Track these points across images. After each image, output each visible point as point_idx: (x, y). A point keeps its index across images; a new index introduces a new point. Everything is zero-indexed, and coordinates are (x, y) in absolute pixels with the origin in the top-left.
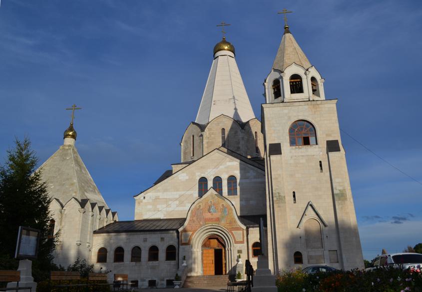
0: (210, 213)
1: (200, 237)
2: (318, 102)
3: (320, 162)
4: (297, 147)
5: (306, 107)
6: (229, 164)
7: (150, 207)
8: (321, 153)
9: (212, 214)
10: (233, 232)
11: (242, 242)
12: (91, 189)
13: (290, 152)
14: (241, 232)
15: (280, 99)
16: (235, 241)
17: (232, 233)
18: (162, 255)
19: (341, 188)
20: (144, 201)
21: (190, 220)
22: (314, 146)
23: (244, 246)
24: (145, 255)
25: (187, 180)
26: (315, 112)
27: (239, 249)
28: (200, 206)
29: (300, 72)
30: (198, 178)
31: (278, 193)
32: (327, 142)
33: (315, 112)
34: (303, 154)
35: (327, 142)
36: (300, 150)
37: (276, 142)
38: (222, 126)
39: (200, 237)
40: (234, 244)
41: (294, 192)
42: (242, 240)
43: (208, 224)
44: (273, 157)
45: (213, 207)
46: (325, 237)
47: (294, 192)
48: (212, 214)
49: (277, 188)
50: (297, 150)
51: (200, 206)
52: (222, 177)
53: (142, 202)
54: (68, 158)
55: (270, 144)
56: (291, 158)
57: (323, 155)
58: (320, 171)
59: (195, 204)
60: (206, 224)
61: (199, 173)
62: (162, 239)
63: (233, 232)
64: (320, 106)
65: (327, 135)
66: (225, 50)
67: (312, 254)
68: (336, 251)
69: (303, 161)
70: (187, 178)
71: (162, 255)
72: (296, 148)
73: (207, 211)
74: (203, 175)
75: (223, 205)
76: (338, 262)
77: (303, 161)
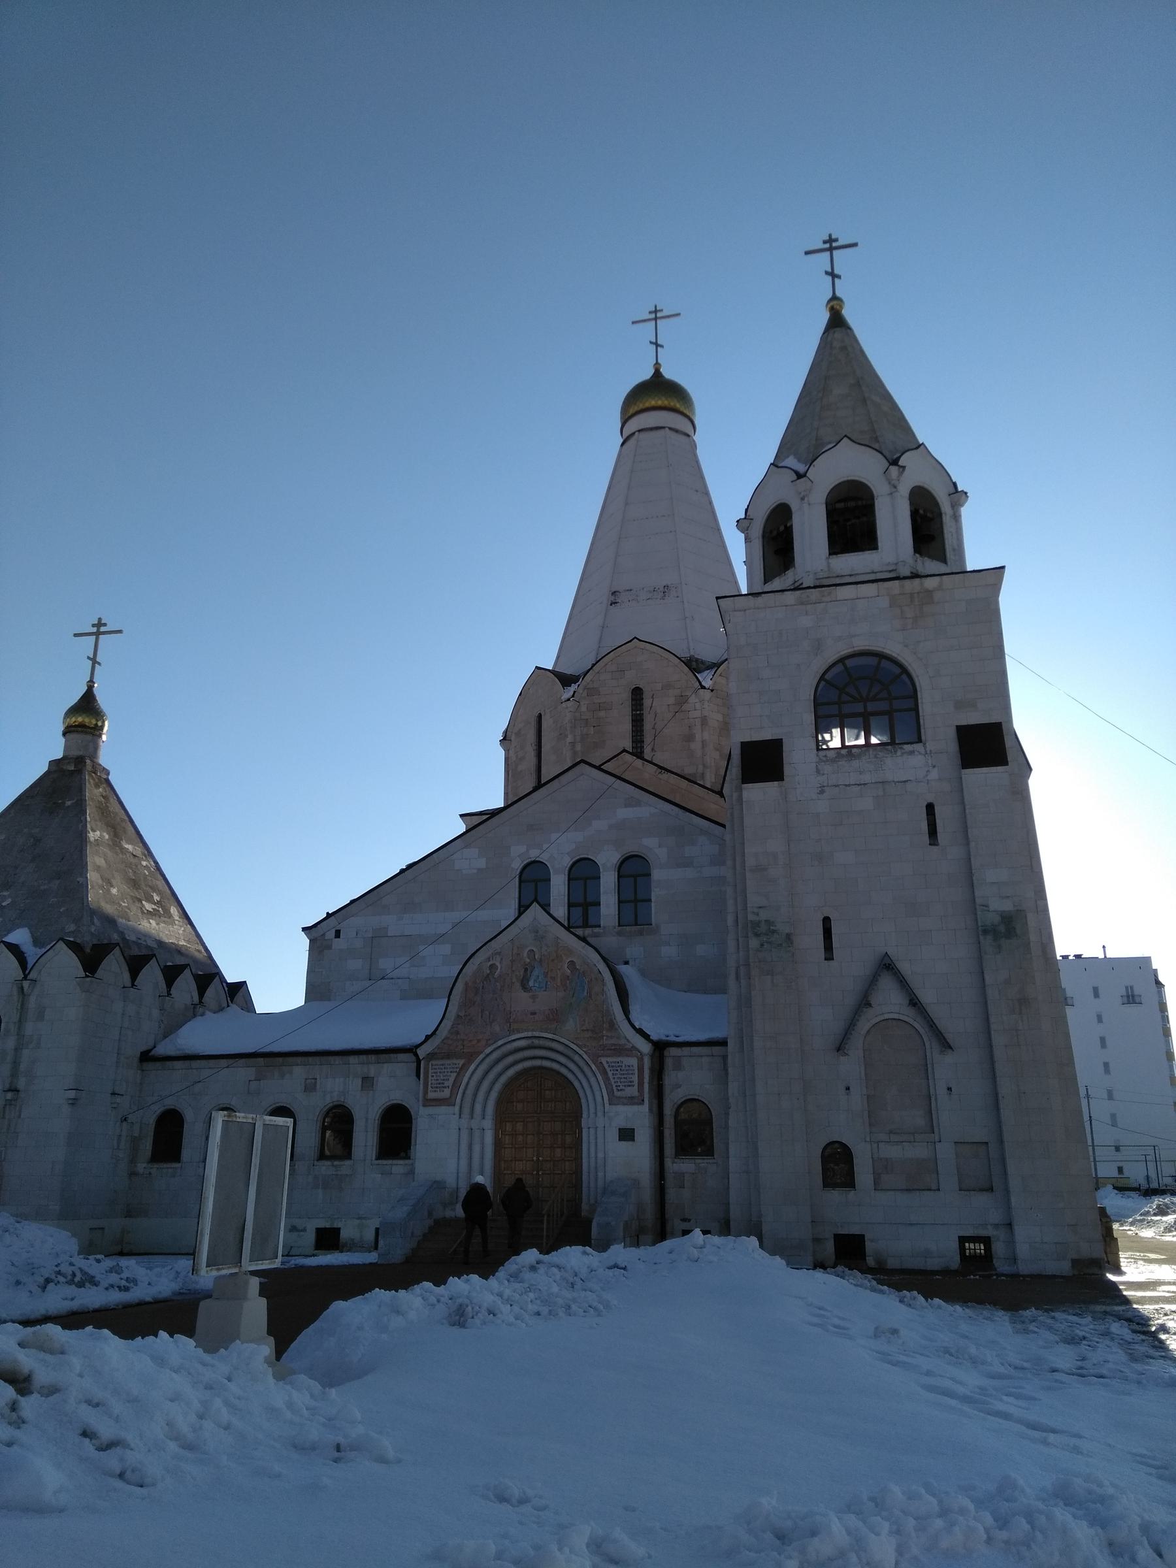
0: (525, 987)
1: (491, 1076)
2: (930, 583)
6: (623, 813)
7: (355, 964)
8: (934, 774)
9: (534, 997)
10: (604, 1060)
11: (631, 1101)
12: (148, 907)
13: (818, 771)
14: (634, 1062)
15: (788, 579)
16: (611, 1093)
17: (600, 1066)
18: (365, 1138)
19: (1007, 906)
20: (339, 944)
21: (458, 1016)
22: (907, 747)
23: (640, 1117)
25: (479, 870)
27: (624, 1125)
28: (493, 967)
30: (517, 865)
32: (960, 729)
34: (867, 778)
35: (960, 729)
37: (766, 735)
38: (632, 678)
39: (491, 1076)
40: (607, 1105)
41: (827, 921)
42: (633, 1091)
43: (519, 1032)
44: (757, 793)
45: (536, 973)
46: (941, 1091)
47: (827, 921)
48: (534, 997)
51: (493, 967)
52: (600, 860)
53: (329, 947)
54: (69, 803)
55: (744, 745)
56: (822, 792)
58: (926, 838)
60: (511, 1031)
61: (523, 849)
62: (368, 1082)
63: (604, 1060)
65: (960, 705)
67: (892, 1152)
68: (987, 1143)
70: (482, 863)
71: (365, 1138)
73: (518, 985)
74: (534, 854)
75: (572, 962)
76: (991, 1189)
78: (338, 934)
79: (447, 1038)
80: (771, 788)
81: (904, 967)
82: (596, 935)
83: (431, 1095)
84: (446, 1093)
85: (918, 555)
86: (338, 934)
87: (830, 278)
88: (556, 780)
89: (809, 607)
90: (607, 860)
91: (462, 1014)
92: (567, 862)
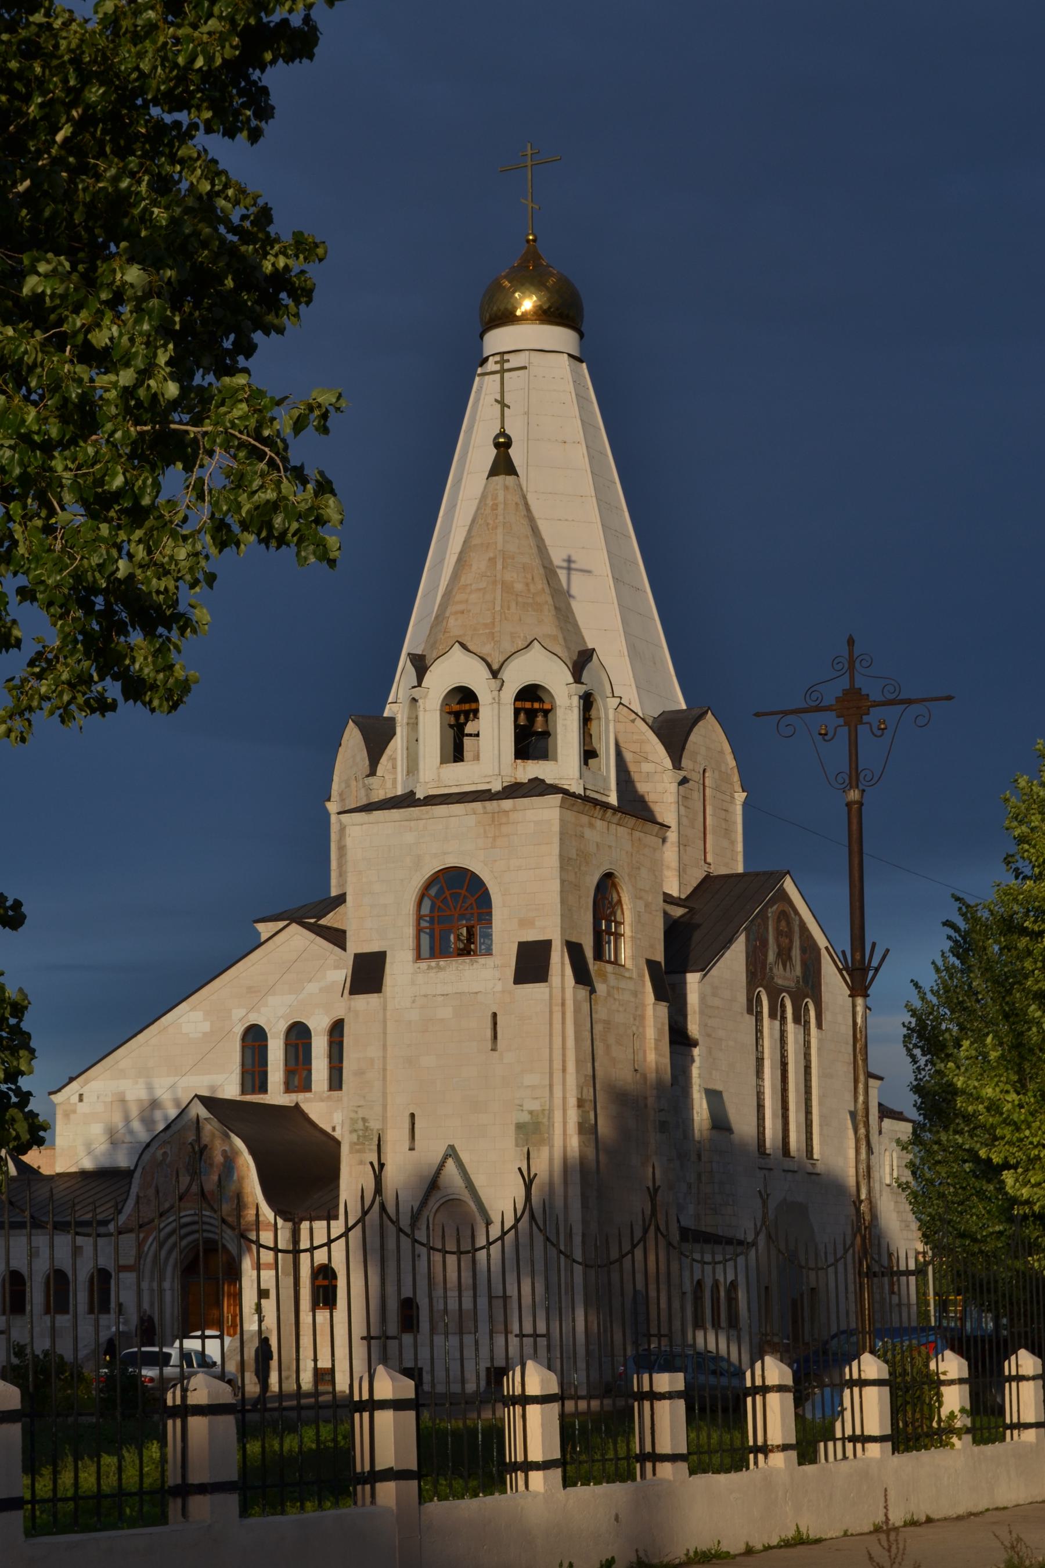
3: (495, 1015)
4: (433, 963)
5: (471, 820)
8: (499, 987)
20: (82, 1108)
24: (36, 1296)
25: (205, 1034)
26: (495, 838)
29: (478, 679)
30: (239, 1030)
31: (364, 1120)
32: (521, 945)
33: (495, 838)
35: (521, 945)
36: (441, 975)
37: (374, 947)
49: (362, 1103)
50: (432, 974)
51: (165, 1153)
53: (74, 1112)
56: (414, 1002)
57: (503, 992)
59: (152, 1149)
64: (513, 816)
65: (525, 923)
66: (524, 318)
69: (446, 1012)
70: (206, 1027)
72: (429, 968)
74: (254, 1019)
77: (446, 1012)
78: (81, 1100)
79: (130, 1215)
80: (373, 999)
81: (465, 1157)
82: (307, 1100)
83: (122, 1262)
84: (131, 1261)
85: (519, 761)
86: (81, 1098)
87: (498, 406)
88: (271, 941)
89: (413, 823)
90: (319, 1026)
91: (141, 1195)
92: (282, 1026)
